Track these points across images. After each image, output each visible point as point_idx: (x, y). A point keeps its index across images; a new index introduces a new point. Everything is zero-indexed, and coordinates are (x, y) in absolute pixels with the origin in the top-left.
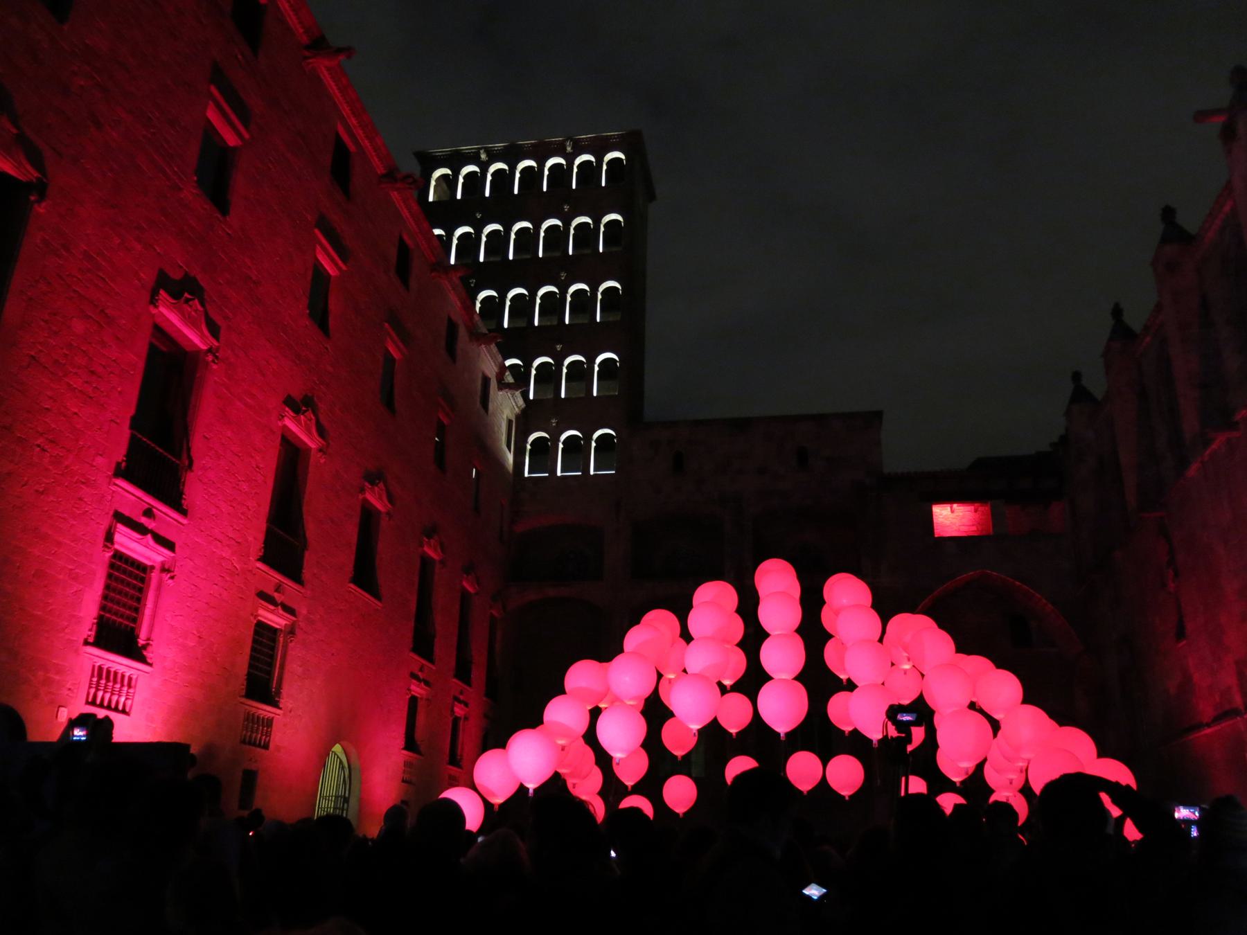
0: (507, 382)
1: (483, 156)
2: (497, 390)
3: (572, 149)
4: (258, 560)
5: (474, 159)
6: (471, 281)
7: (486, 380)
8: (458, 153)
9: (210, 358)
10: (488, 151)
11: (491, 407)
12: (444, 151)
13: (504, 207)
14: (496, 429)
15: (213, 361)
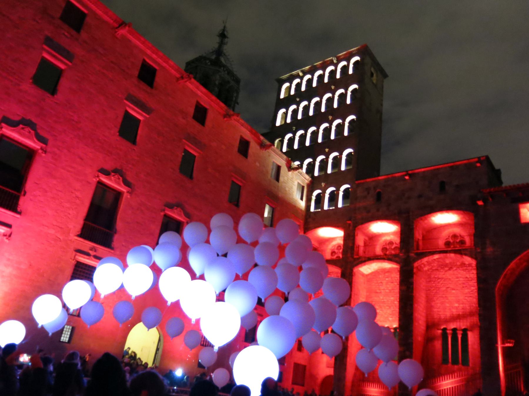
0: (293, 167)
1: (301, 74)
2: (288, 171)
3: (337, 60)
4: (76, 236)
5: (298, 76)
6: (293, 128)
7: (279, 168)
8: (291, 75)
9: (40, 151)
10: (302, 71)
11: (281, 179)
12: (287, 76)
13: (310, 93)
14: (287, 189)
15: (42, 153)
